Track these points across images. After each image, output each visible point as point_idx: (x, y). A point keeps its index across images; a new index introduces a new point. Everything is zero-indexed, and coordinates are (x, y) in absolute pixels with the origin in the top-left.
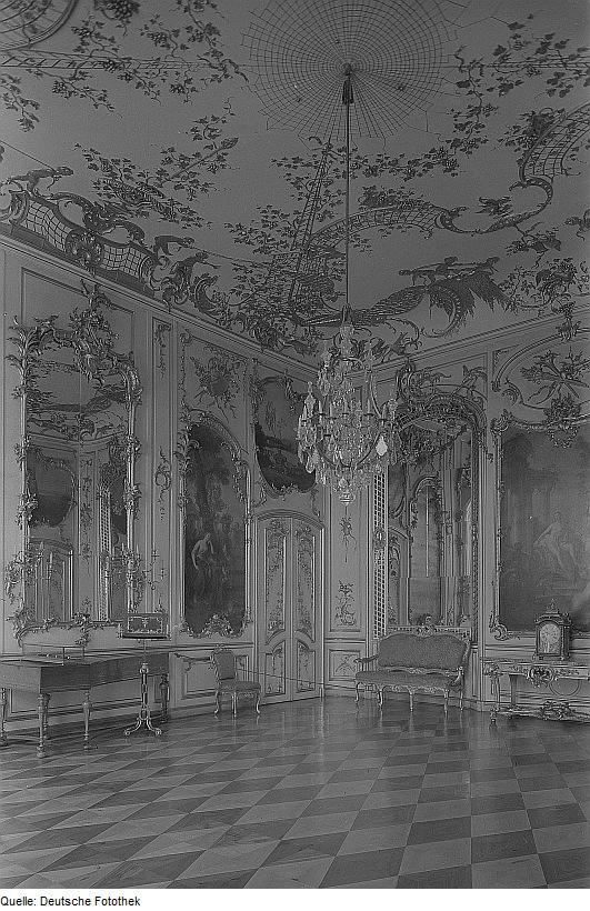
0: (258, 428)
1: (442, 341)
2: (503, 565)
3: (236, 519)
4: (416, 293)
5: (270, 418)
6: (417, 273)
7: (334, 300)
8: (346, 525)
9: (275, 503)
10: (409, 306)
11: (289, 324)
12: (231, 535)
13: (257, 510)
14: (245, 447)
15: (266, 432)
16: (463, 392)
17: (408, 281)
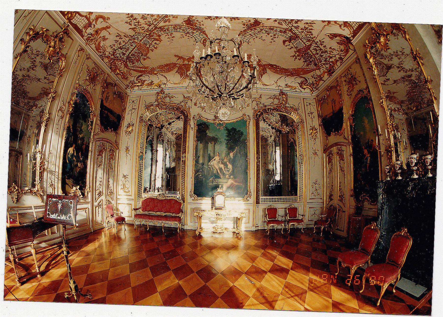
0: (102, 101)
1: (176, 86)
2: (197, 171)
3: (86, 140)
4: (175, 65)
5: (107, 98)
6: (180, 58)
7: (144, 59)
8: (127, 149)
9: (103, 135)
10: (169, 70)
11: (123, 66)
12: (84, 147)
13: (96, 137)
14: (95, 109)
15: (104, 102)
16: (183, 104)
17: (174, 60)
